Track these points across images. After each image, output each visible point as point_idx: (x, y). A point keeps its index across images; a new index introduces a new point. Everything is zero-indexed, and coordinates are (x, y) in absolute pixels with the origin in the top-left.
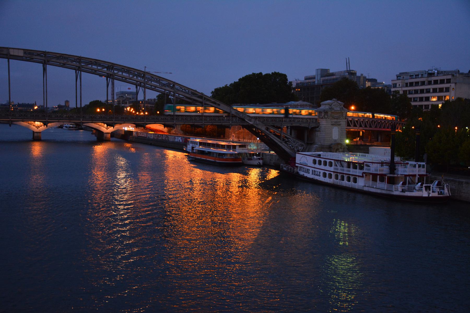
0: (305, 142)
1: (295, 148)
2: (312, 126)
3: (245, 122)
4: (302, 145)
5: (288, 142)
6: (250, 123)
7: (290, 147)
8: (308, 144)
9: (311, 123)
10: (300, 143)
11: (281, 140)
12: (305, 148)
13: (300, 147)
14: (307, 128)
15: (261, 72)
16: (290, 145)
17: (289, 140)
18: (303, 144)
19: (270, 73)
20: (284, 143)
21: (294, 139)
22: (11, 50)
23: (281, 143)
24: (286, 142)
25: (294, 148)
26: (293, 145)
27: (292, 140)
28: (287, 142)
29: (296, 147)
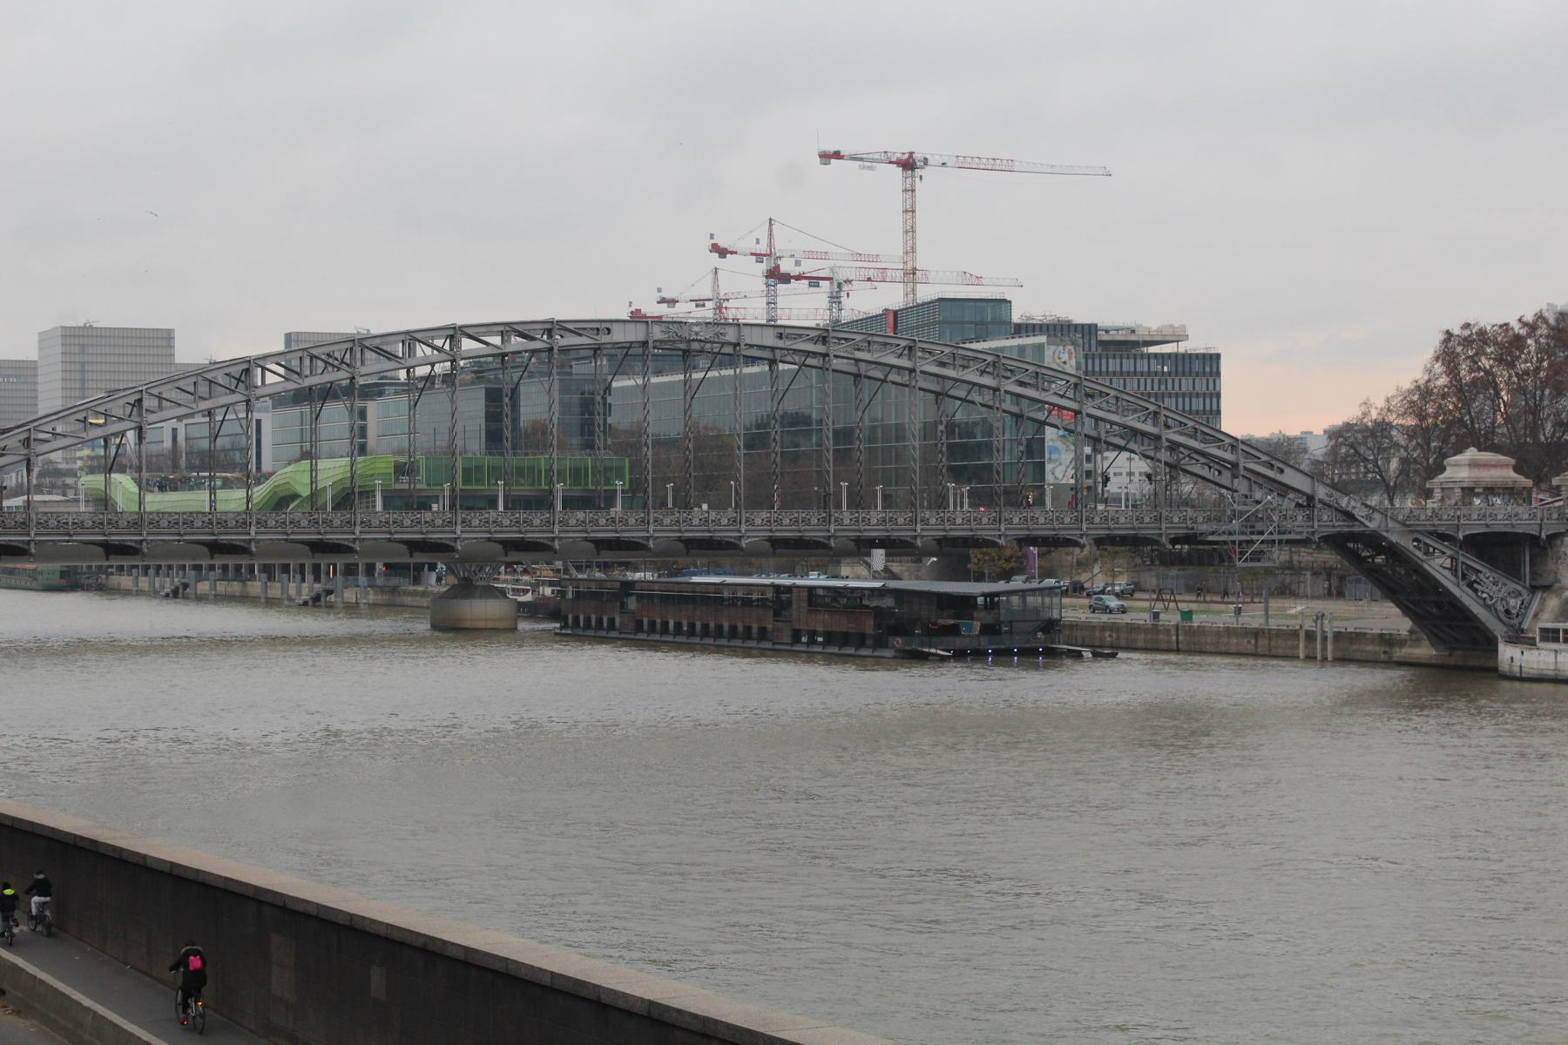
0: (1525, 582)
1: (1499, 603)
2: (1550, 532)
3: (1356, 523)
5: (1479, 584)
6: (1368, 527)
7: (1485, 599)
8: (1534, 589)
9: (1545, 520)
10: (1512, 586)
11: (1456, 576)
12: (1525, 601)
13: (1514, 598)
14: (1533, 540)
15: (1209, 364)
16: (1483, 592)
17: (1481, 576)
18: (1520, 588)
20: (1468, 590)
21: (1495, 575)
22: (745, 331)
23: (1458, 586)
24: (1470, 585)
25: (1496, 602)
26: (1491, 594)
27: (1488, 578)
28: (1476, 586)
29: (1502, 599)
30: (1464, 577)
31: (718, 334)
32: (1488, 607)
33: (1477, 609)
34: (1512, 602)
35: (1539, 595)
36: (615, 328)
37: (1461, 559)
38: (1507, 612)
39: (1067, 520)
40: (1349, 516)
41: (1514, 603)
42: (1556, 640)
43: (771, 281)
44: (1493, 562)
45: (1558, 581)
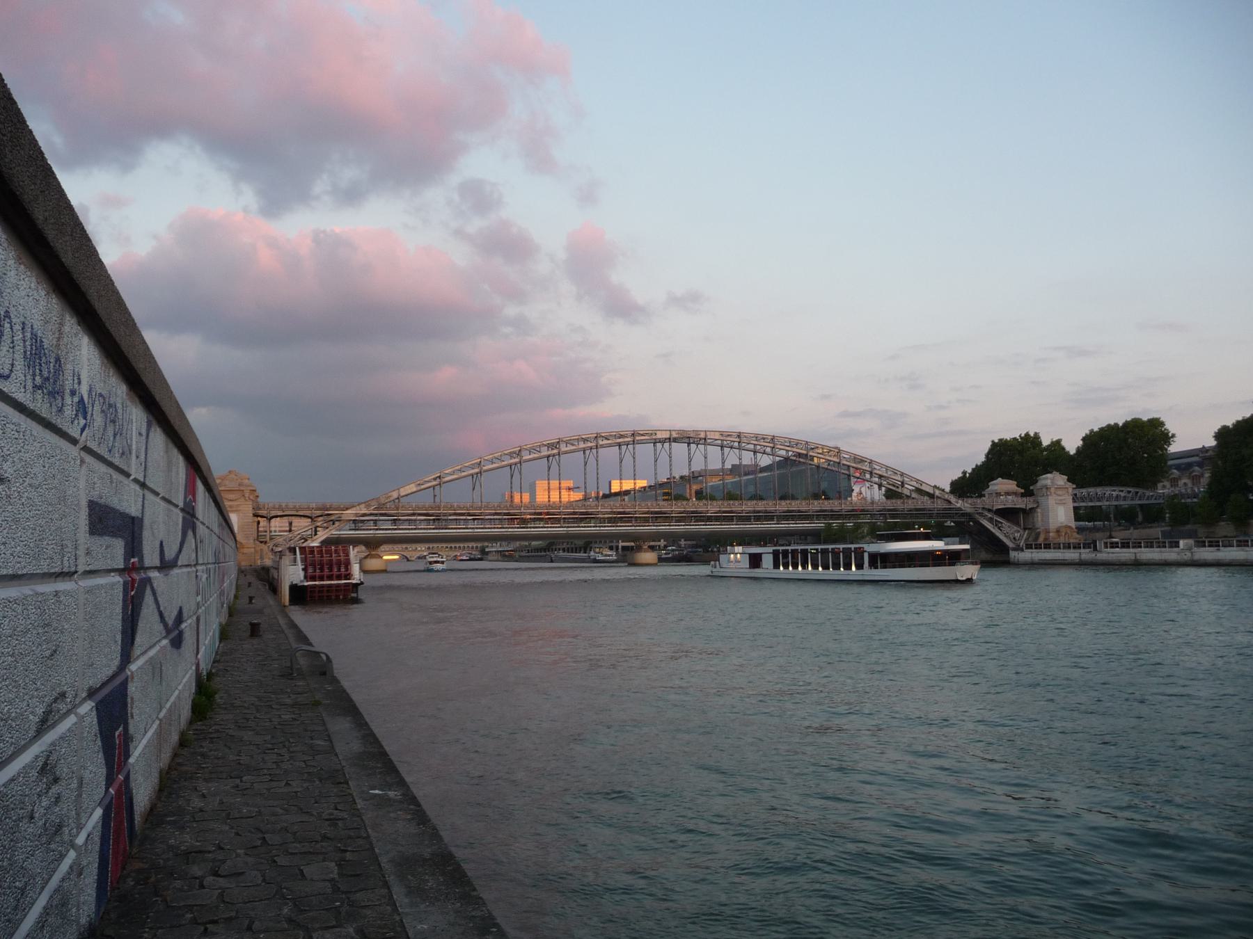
4: (1019, 531)
8: (1025, 529)
10: (1016, 528)
14: (1024, 511)
18: (1019, 529)
19: (1043, 443)
22: (708, 433)
24: (999, 528)
30: (996, 525)
31: (697, 435)
32: (1006, 536)
33: (1002, 537)
34: (1016, 535)
35: (1027, 532)
36: (658, 432)
37: (995, 518)
38: (1014, 538)
39: (836, 504)
40: (950, 502)
41: (1017, 535)
42: (1032, 548)
43: (35, 389)
44: (1008, 520)
45: (1034, 526)
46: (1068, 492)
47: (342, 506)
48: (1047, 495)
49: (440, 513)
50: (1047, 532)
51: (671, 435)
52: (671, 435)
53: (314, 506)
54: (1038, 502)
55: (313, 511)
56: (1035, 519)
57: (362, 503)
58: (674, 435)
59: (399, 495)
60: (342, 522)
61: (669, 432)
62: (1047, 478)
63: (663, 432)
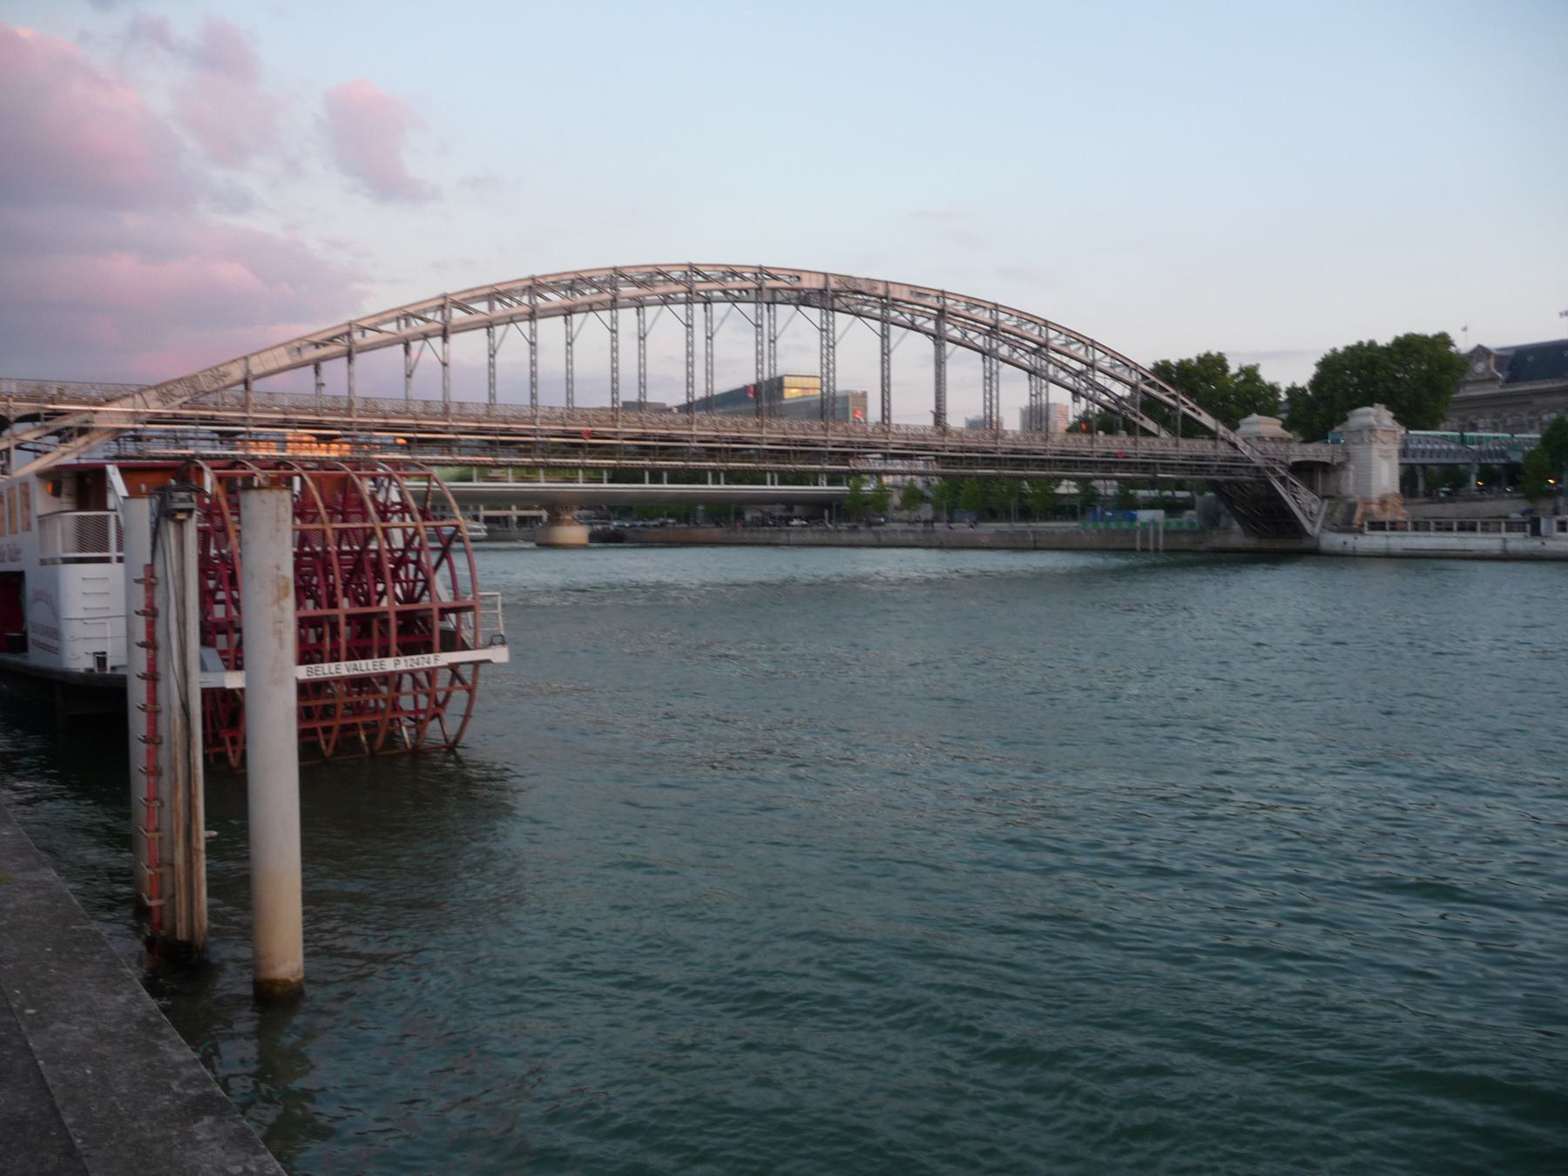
36: (804, 276)
38: (1311, 513)
42: (1384, 529)
46: (1395, 439)
47: (93, 393)
48: (1370, 441)
49: (350, 423)
50: (1368, 502)
51: (827, 282)
52: (827, 282)
53: (14, 388)
54: (1348, 454)
55: (12, 403)
56: (1342, 482)
57: (150, 388)
58: (833, 285)
59: (248, 371)
60: (94, 434)
61: (822, 278)
62: (1369, 414)
63: (814, 276)
